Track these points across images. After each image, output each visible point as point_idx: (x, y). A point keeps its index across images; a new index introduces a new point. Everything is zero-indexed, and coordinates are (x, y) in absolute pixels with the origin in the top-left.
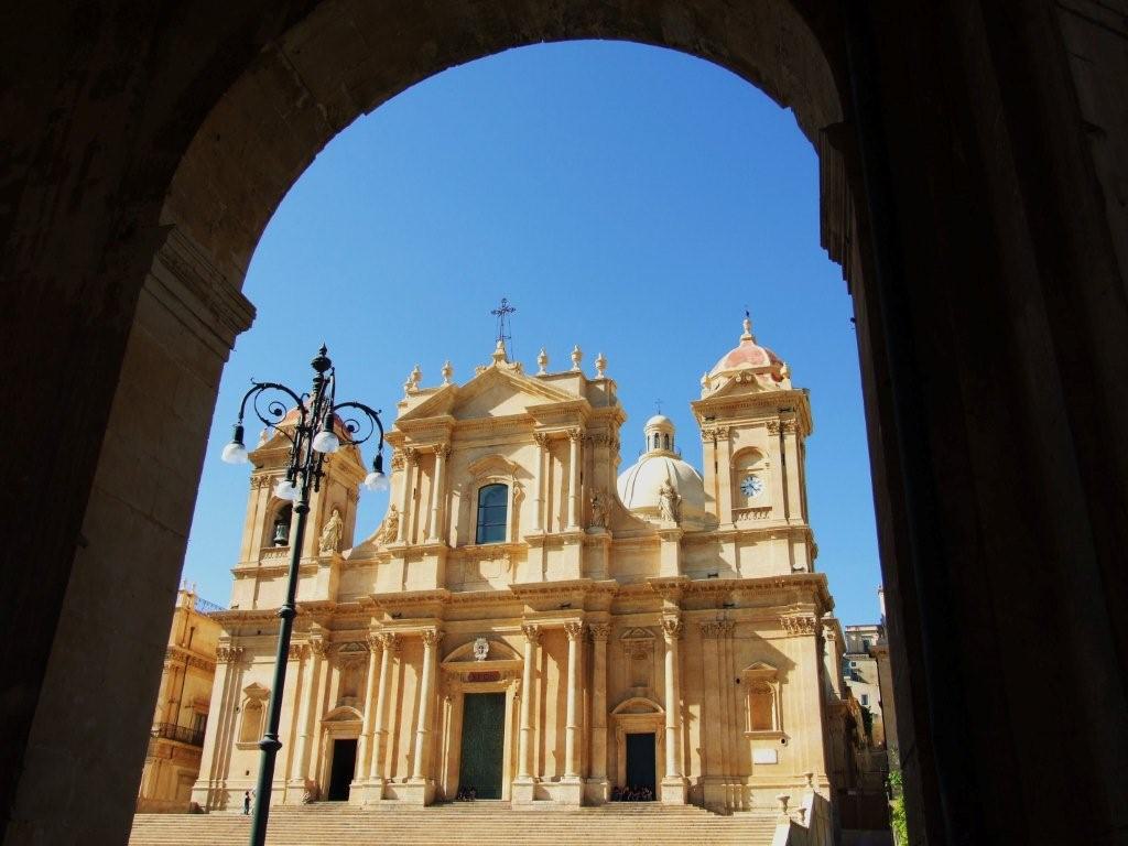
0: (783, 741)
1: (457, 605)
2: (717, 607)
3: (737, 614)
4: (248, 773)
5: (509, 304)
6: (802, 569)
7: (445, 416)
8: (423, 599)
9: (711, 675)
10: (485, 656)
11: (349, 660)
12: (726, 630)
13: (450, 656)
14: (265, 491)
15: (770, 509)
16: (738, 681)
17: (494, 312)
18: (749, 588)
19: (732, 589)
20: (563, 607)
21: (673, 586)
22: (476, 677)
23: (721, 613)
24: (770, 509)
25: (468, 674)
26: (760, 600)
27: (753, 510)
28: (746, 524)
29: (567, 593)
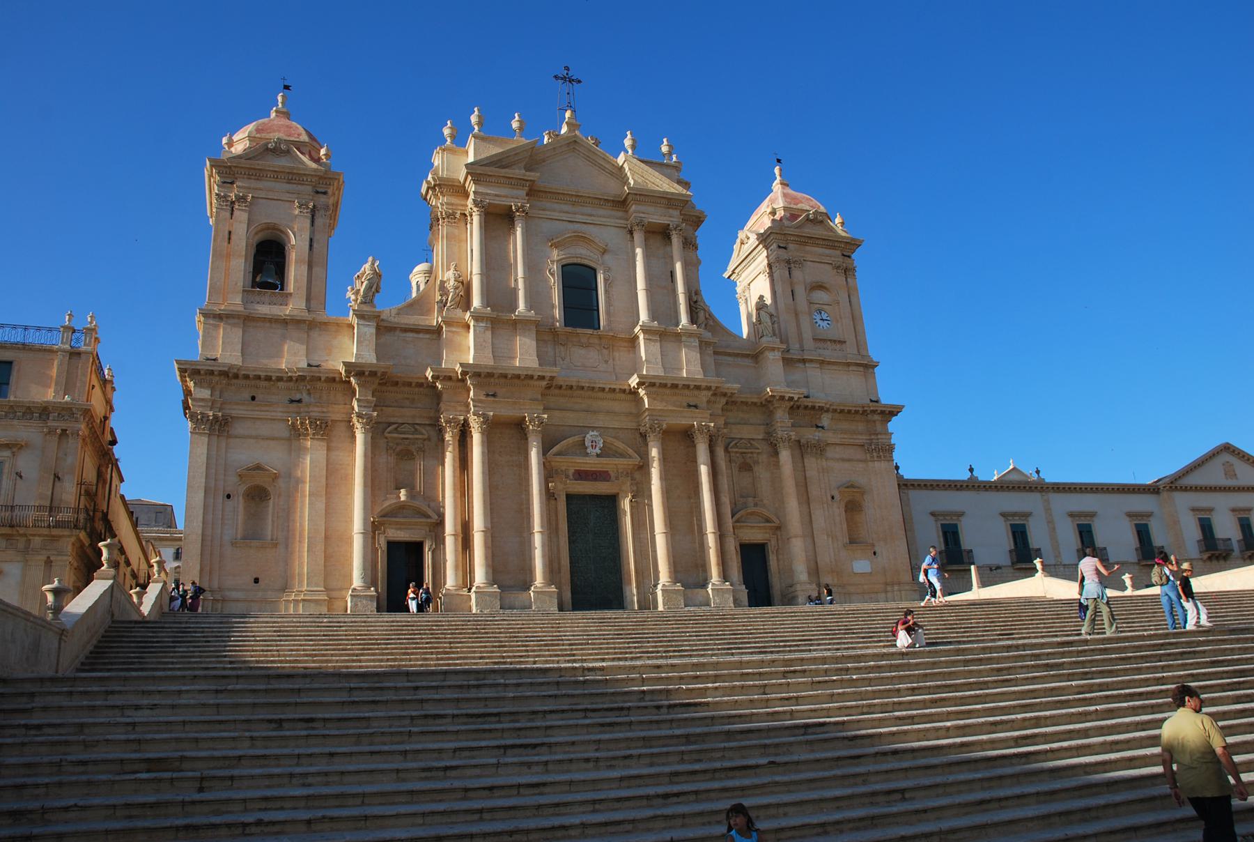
0: (875, 553)
1: (557, 391)
2: (812, 427)
3: (830, 437)
4: (256, 581)
5: (573, 73)
7: (518, 172)
8: (531, 377)
9: (814, 491)
10: (599, 452)
11: (397, 444)
12: (819, 449)
13: (555, 449)
14: (241, 215)
15: (845, 342)
16: (833, 498)
18: (842, 411)
19: (828, 411)
20: (689, 406)
21: (791, 399)
23: (818, 434)
25: (571, 471)
26: (845, 425)
27: (830, 340)
28: (829, 353)
29: (696, 392)
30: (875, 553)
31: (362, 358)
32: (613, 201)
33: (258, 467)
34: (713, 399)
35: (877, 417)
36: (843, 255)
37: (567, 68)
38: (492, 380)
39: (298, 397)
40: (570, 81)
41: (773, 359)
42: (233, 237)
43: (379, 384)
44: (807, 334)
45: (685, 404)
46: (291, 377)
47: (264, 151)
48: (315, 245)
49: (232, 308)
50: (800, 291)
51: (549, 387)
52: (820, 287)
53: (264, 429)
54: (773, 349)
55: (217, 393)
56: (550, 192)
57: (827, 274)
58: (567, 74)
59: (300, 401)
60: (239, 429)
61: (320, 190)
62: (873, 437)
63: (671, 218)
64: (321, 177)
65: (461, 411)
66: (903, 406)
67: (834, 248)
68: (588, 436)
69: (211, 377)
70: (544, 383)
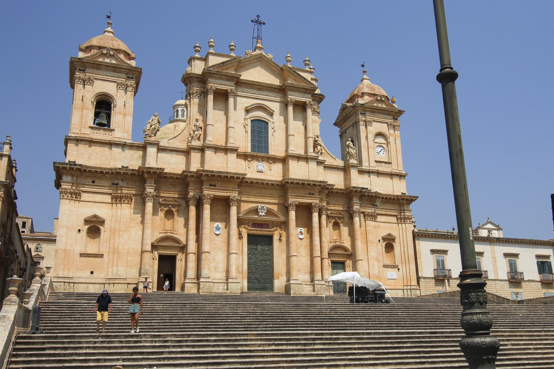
0: (399, 269)
1: (245, 184)
5: (262, 19)
6: (405, 194)
7: (232, 72)
9: (370, 237)
10: (263, 214)
11: (166, 207)
12: (373, 217)
16: (379, 241)
17: (252, 21)
18: (387, 198)
22: (257, 224)
24: (391, 163)
27: (384, 162)
29: (314, 187)
30: (399, 269)
31: (149, 164)
32: (278, 88)
33: (95, 216)
34: (322, 190)
35: (404, 202)
36: (394, 118)
37: (258, 16)
38: (214, 178)
39: (117, 182)
40: (259, 23)
41: (353, 171)
42: (85, 99)
43: (158, 177)
44: (372, 160)
45: (308, 193)
46: (113, 172)
47: (101, 54)
48: (127, 105)
49: (82, 136)
50: (371, 137)
51: (241, 182)
52: (379, 134)
53: (99, 198)
54: (353, 166)
55: (75, 179)
56: (246, 83)
57: (383, 128)
58: (258, 19)
59: (117, 184)
60: (85, 196)
61: (130, 76)
62: (402, 211)
63: (307, 99)
64: (130, 70)
65: (198, 192)
66: (418, 197)
67: (389, 115)
68: (259, 207)
69: (72, 171)
70: (239, 180)
